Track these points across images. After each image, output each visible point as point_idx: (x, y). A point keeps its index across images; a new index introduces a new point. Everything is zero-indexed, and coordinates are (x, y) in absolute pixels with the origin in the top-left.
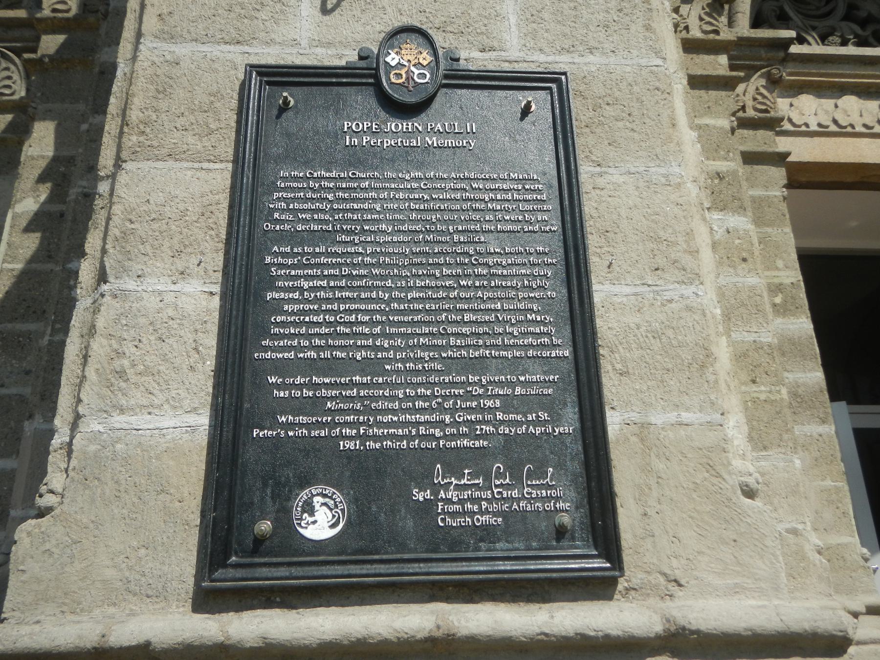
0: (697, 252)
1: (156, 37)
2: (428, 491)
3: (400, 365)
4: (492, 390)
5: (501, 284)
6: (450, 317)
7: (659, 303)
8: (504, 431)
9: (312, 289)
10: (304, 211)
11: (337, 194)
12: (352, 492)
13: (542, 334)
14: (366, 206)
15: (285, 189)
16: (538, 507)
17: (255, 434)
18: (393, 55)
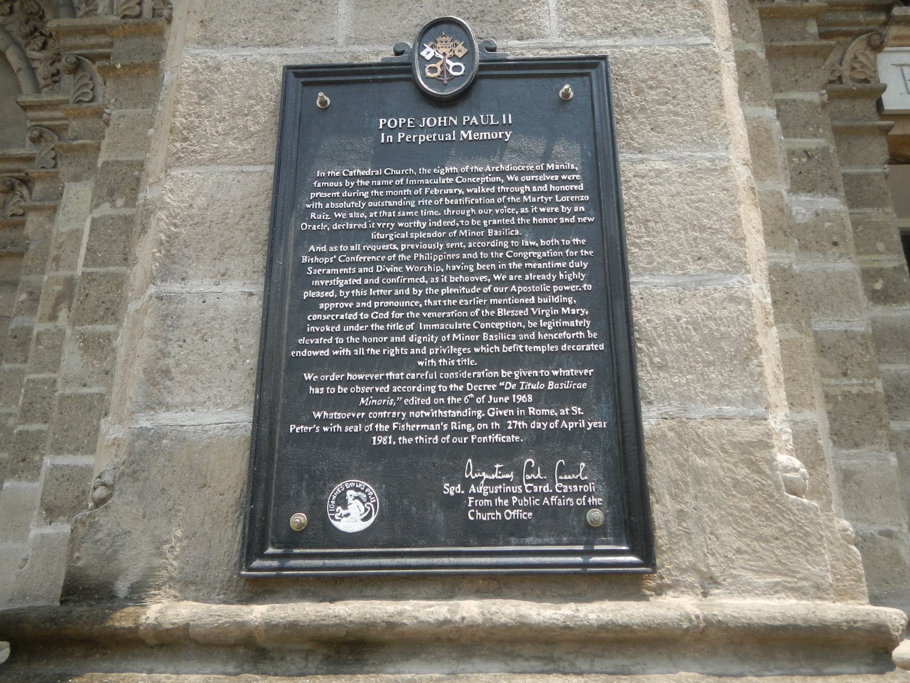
0: (744, 239)
1: (198, 44)
2: (459, 485)
3: (432, 361)
4: (524, 385)
5: (536, 278)
6: (483, 312)
7: (701, 294)
8: (536, 426)
9: (346, 287)
11: (372, 192)
12: (384, 486)
13: (577, 329)
14: (400, 203)
15: (324, 189)
16: (569, 502)
17: (291, 429)
18: (428, 48)
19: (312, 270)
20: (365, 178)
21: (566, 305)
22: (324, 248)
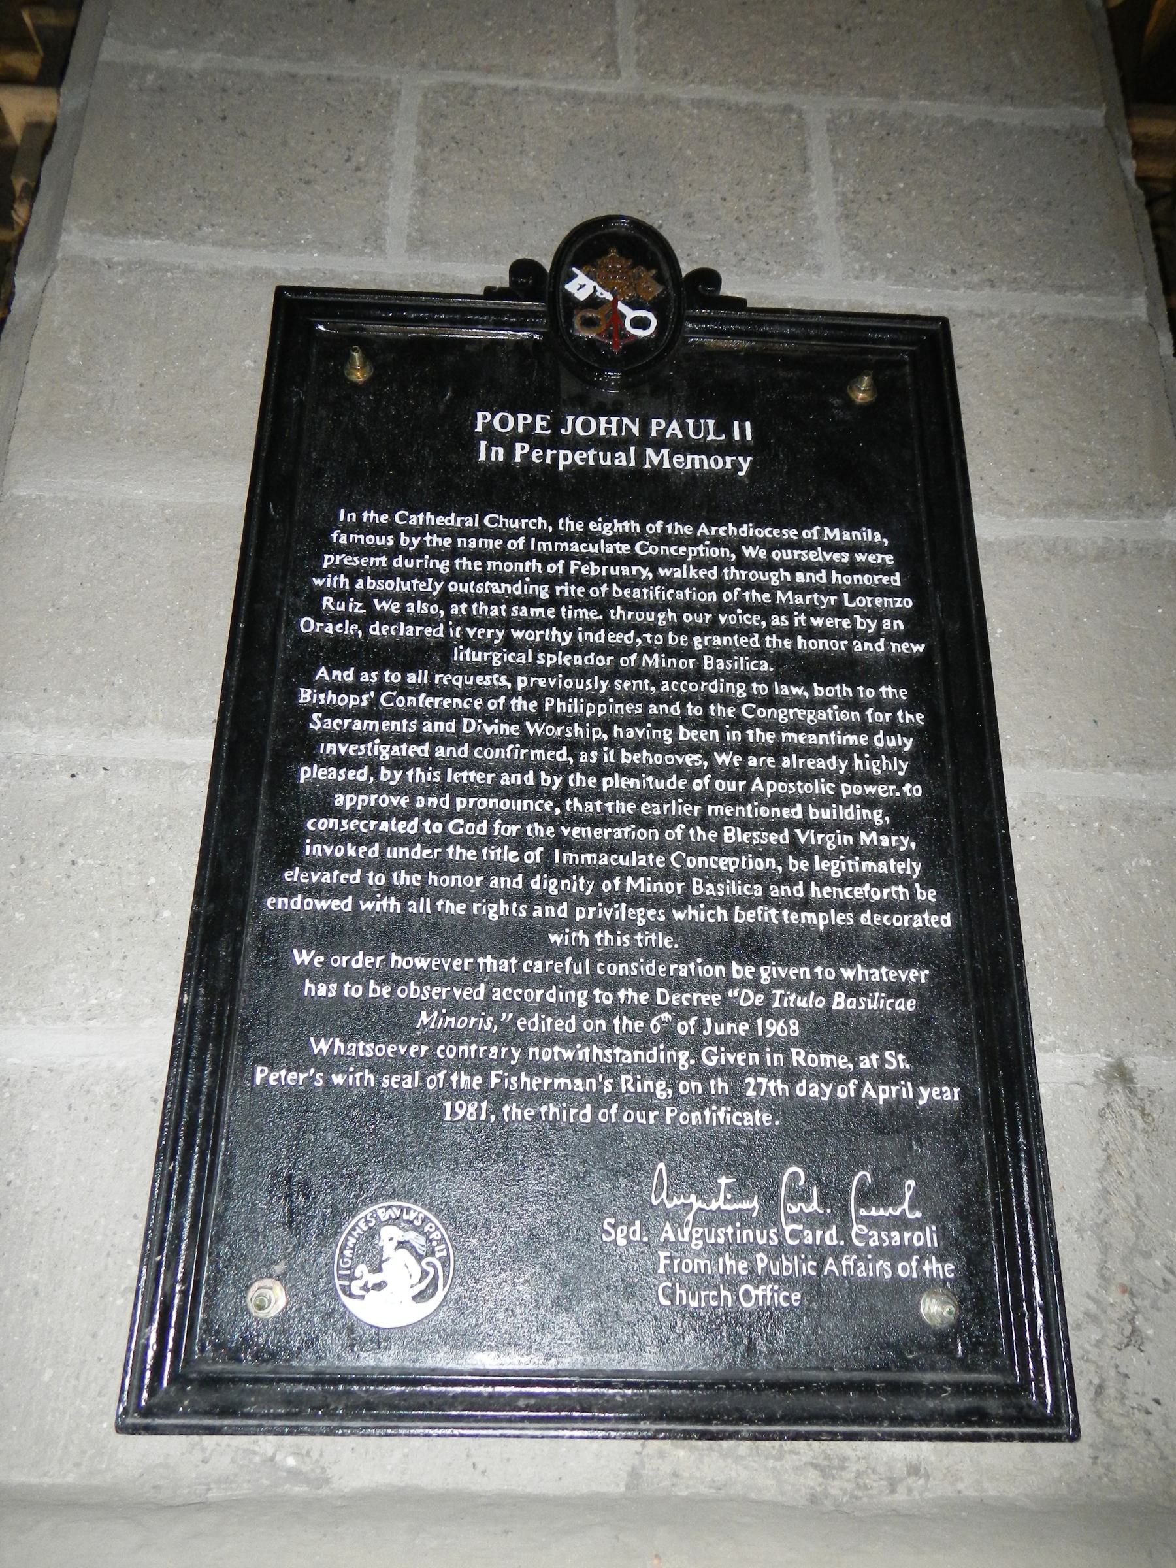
3: (581, 934)
6: (692, 832)
8: (808, 1090)
9: (397, 764)
10: (384, 596)
17: (259, 1078)
19: (321, 719)
20: (443, 532)
21: (869, 826)
22: (349, 675)
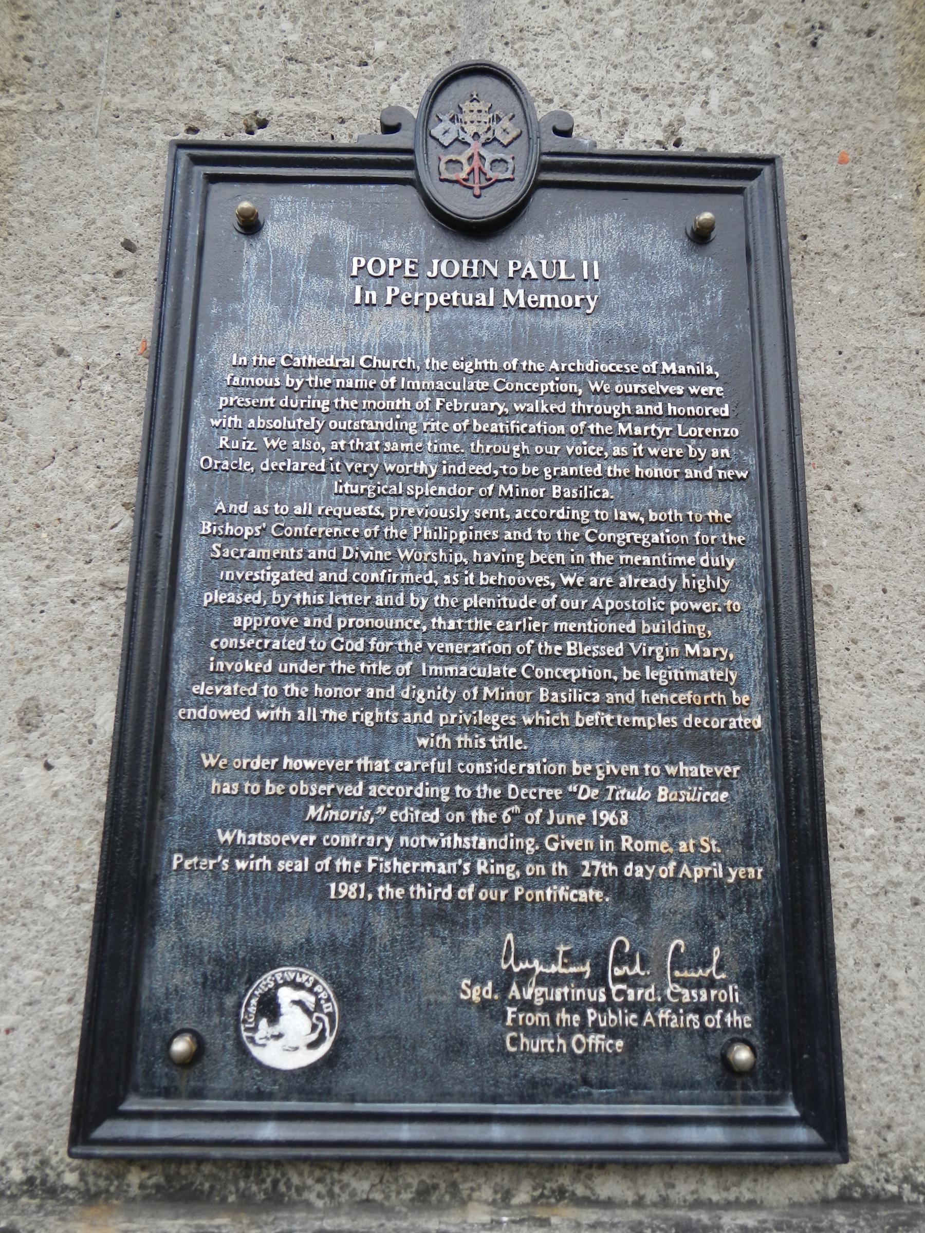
2: (490, 984)
3: (444, 738)
4: (615, 791)
5: (639, 583)
6: (540, 646)
8: (634, 871)
13: (714, 684)
19: (220, 549)
